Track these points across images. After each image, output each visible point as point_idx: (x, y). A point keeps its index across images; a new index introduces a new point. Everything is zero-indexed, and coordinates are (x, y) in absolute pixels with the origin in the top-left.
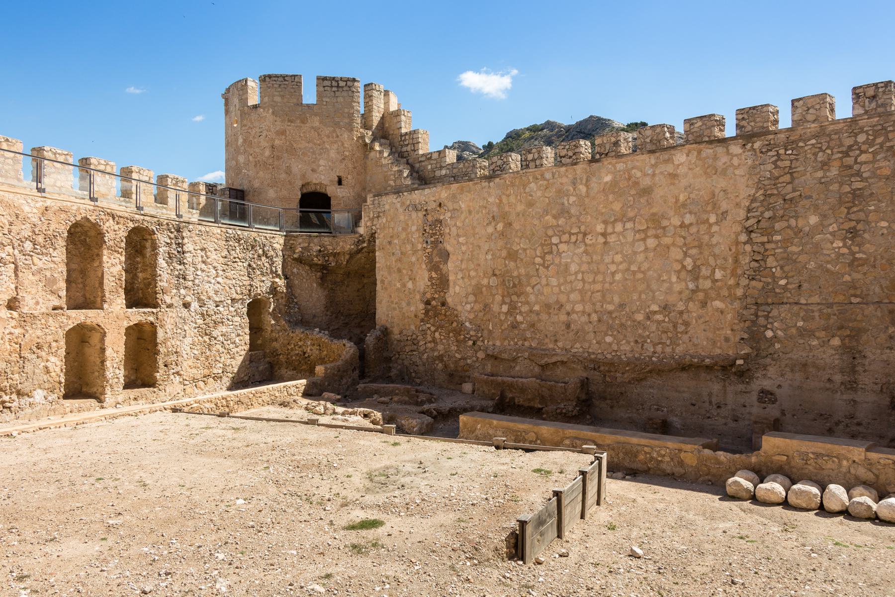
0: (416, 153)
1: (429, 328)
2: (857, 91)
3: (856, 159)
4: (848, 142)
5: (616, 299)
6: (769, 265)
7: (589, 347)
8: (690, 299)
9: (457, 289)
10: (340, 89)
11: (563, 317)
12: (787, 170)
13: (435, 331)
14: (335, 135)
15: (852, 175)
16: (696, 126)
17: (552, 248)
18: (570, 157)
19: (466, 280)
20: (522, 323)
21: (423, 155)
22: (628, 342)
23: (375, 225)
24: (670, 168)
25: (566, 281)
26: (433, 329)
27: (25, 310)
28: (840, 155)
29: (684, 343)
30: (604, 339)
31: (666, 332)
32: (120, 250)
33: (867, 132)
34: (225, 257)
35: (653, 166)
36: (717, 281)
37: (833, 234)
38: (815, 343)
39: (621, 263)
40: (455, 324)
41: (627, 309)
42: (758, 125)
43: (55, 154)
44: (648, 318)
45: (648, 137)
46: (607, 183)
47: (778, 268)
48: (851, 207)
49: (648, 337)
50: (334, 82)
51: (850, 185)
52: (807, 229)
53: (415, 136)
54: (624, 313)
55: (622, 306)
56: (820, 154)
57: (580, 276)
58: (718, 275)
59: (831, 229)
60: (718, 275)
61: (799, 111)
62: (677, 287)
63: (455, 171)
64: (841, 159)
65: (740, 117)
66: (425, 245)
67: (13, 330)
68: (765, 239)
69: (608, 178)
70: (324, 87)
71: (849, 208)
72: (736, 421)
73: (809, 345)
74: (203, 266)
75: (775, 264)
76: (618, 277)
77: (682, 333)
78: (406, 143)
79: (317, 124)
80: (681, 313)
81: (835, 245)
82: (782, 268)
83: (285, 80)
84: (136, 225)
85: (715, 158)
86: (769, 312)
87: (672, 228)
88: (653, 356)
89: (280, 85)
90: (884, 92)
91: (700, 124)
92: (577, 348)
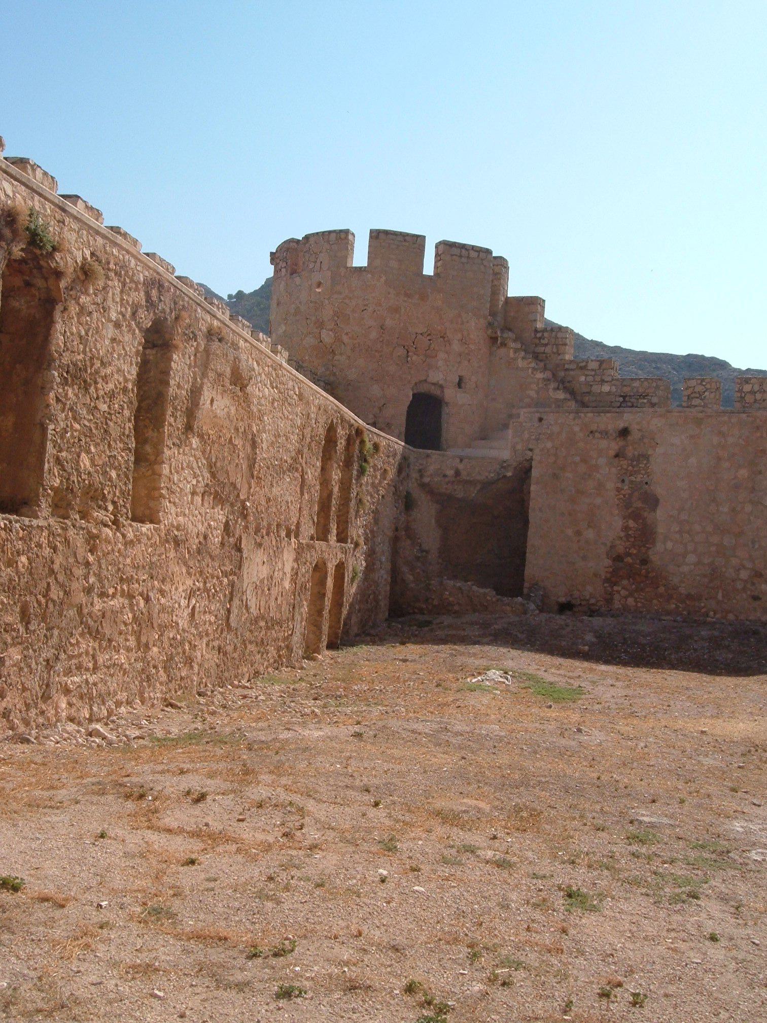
0: (560, 357)
1: (618, 592)
9: (669, 545)
13: (626, 598)
21: (571, 362)
26: (623, 593)
50: (463, 251)
63: (626, 389)
66: (619, 485)
78: (545, 341)
83: (405, 241)
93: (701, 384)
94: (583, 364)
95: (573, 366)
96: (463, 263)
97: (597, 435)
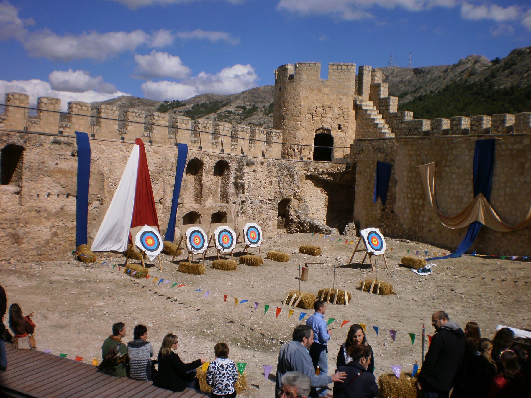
1: (383, 226)
9: (400, 204)
10: (343, 71)
13: (386, 228)
14: (338, 98)
19: (406, 199)
21: (392, 114)
23: (357, 158)
26: (385, 226)
27: (166, 205)
32: (211, 173)
34: (267, 176)
40: (397, 225)
43: (183, 120)
53: (388, 100)
63: (410, 126)
67: (161, 215)
70: (333, 69)
74: (254, 181)
79: (327, 92)
83: (310, 66)
84: (220, 159)
89: (307, 69)
93: (437, 122)
94: (395, 115)
95: (392, 116)
96: (339, 72)
97: (377, 151)
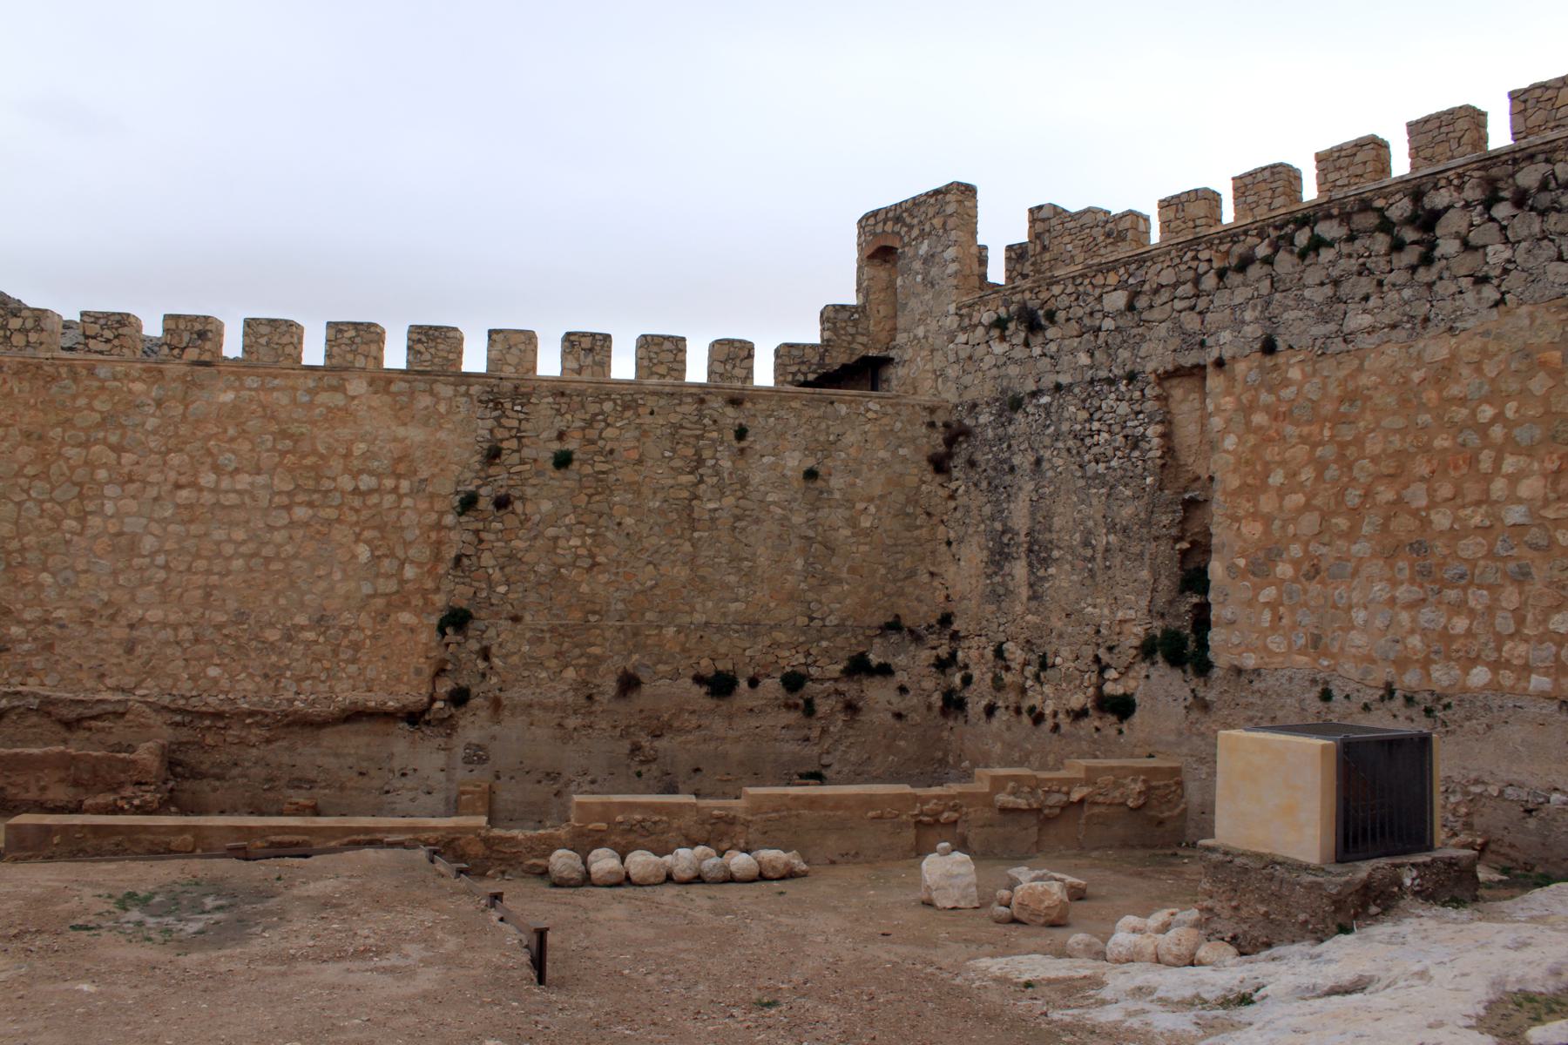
2: (572, 338)
3: (601, 433)
4: (594, 408)
5: (232, 604)
6: (483, 564)
7: (174, 686)
8: (361, 609)
11: (120, 632)
12: (514, 432)
15: (595, 453)
16: (346, 335)
17: (103, 505)
18: (108, 341)
20: (21, 641)
22: (251, 675)
24: (338, 399)
25: (130, 566)
28: (582, 424)
29: (349, 677)
30: (204, 671)
31: (320, 661)
33: (614, 401)
35: (309, 391)
36: (407, 582)
37: (569, 528)
38: (544, 675)
39: (244, 542)
41: (252, 621)
42: (441, 354)
44: (290, 639)
45: (262, 336)
46: (225, 404)
47: (497, 569)
48: (593, 495)
49: (288, 667)
51: (592, 466)
52: (537, 518)
54: (246, 626)
55: (241, 617)
56: (559, 418)
57: (160, 560)
58: (410, 572)
59: (567, 521)
60: (410, 572)
61: (499, 346)
62: (341, 589)
64: (583, 429)
65: (415, 337)
68: (480, 525)
69: (228, 397)
71: (590, 496)
72: (429, 793)
73: (537, 678)
75: (492, 562)
76: (238, 564)
77: (348, 662)
80: (347, 630)
81: (572, 543)
82: (502, 569)
85: (412, 394)
86: (483, 632)
87: (338, 495)
88: (295, 700)
90: (602, 346)
91: (352, 333)
92: (149, 689)
